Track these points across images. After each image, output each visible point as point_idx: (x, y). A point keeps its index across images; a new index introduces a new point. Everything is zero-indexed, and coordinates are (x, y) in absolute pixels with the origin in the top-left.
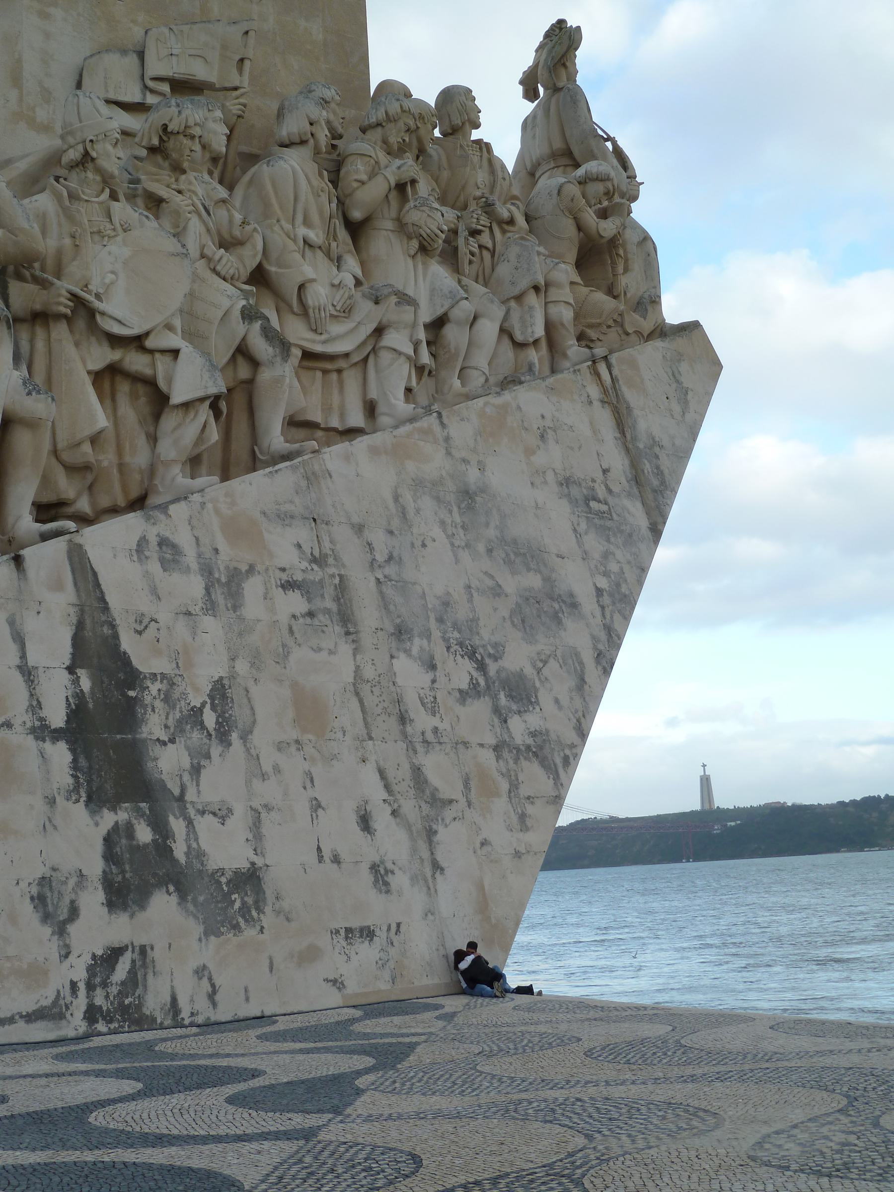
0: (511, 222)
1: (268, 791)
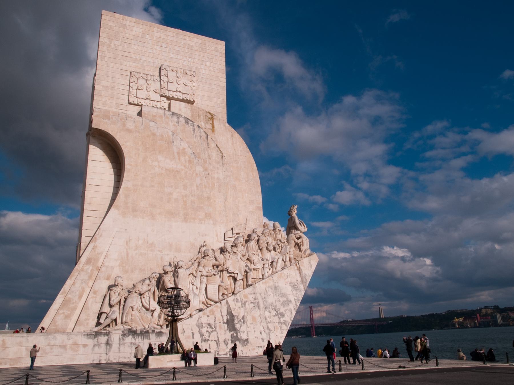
0: (284, 242)
1: (249, 329)
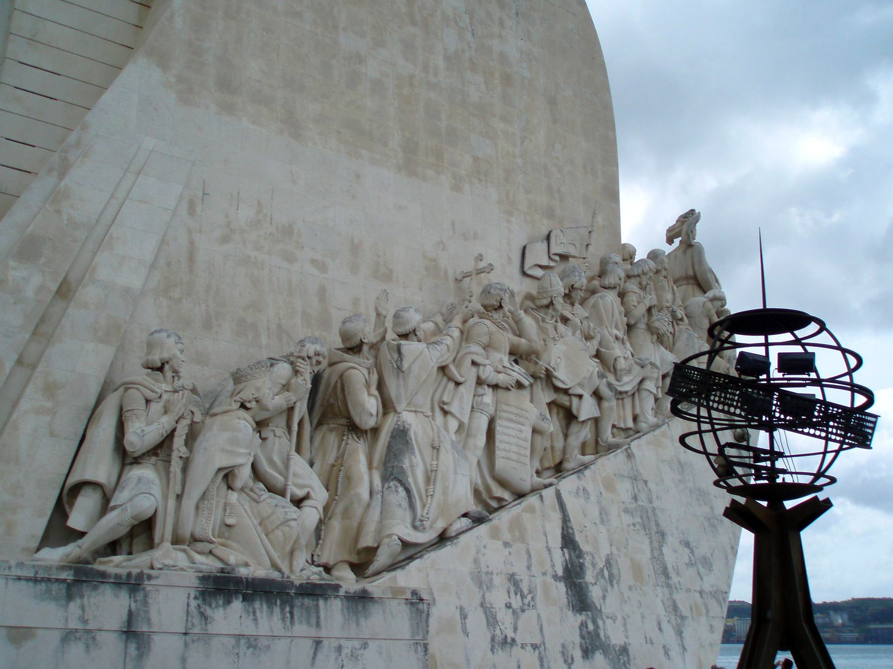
0: (681, 320)
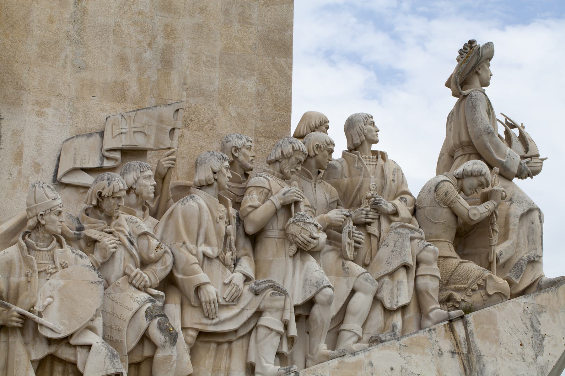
0: (396, 213)
